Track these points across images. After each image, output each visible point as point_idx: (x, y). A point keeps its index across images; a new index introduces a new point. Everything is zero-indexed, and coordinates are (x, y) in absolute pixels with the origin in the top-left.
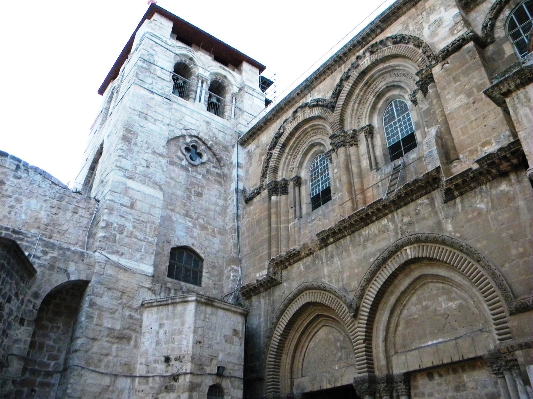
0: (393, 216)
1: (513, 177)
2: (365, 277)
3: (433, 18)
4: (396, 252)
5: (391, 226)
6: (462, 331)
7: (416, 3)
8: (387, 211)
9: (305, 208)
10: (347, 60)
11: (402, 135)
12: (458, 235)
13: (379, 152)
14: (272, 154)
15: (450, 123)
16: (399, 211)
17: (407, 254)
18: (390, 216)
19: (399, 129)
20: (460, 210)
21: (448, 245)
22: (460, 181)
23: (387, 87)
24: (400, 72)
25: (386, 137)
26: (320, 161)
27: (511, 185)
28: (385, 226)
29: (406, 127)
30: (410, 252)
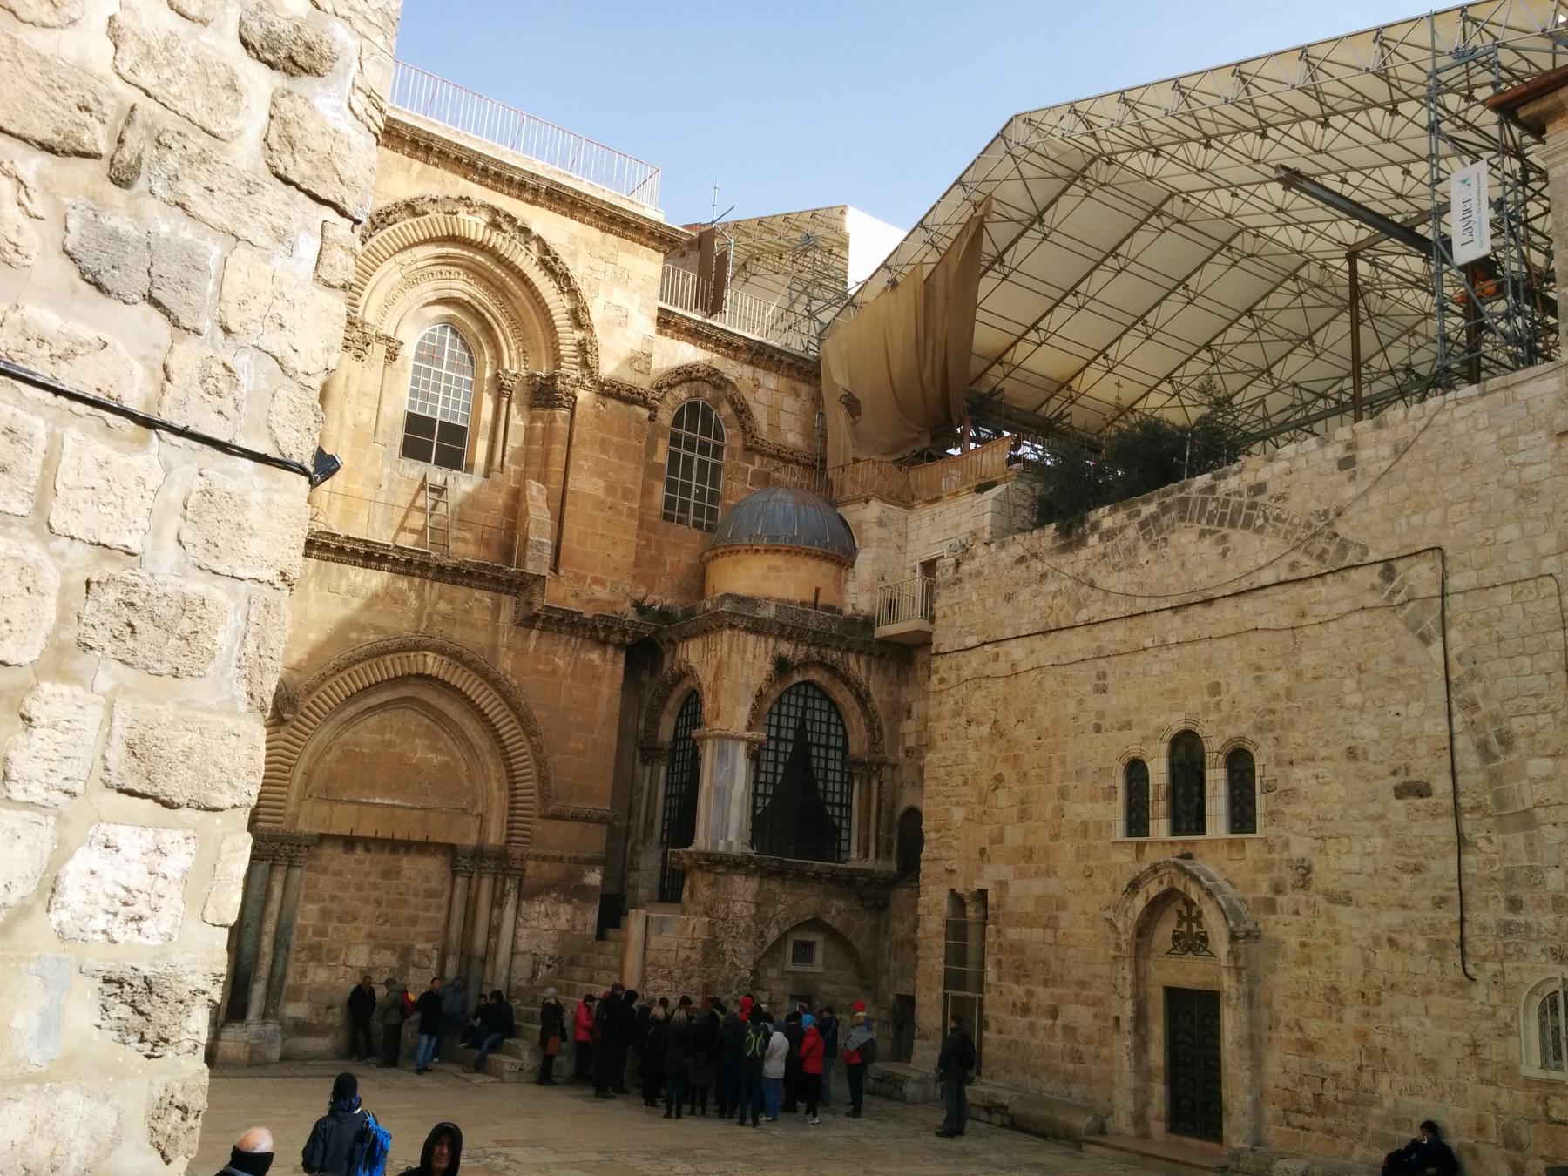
0: (422, 586)
1: (610, 650)
2: (336, 662)
3: (619, 296)
4: (411, 650)
5: (413, 600)
6: (434, 801)
7: (610, 231)
8: (417, 572)
10: (436, 165)
11: (444, 413)
12: (515, 683)
15: (568, 508)
16: (437, 584)
17: (425, 663)
18: (417, 581)
19: (441, 395)
20: (531, 649)
21: (498, 691)
22: (558, 616)
23: (468, 303)
24: (508, 308)
25: (409, 386)
27: (604, 660)
28: (401, 591)
30: (432, 664)
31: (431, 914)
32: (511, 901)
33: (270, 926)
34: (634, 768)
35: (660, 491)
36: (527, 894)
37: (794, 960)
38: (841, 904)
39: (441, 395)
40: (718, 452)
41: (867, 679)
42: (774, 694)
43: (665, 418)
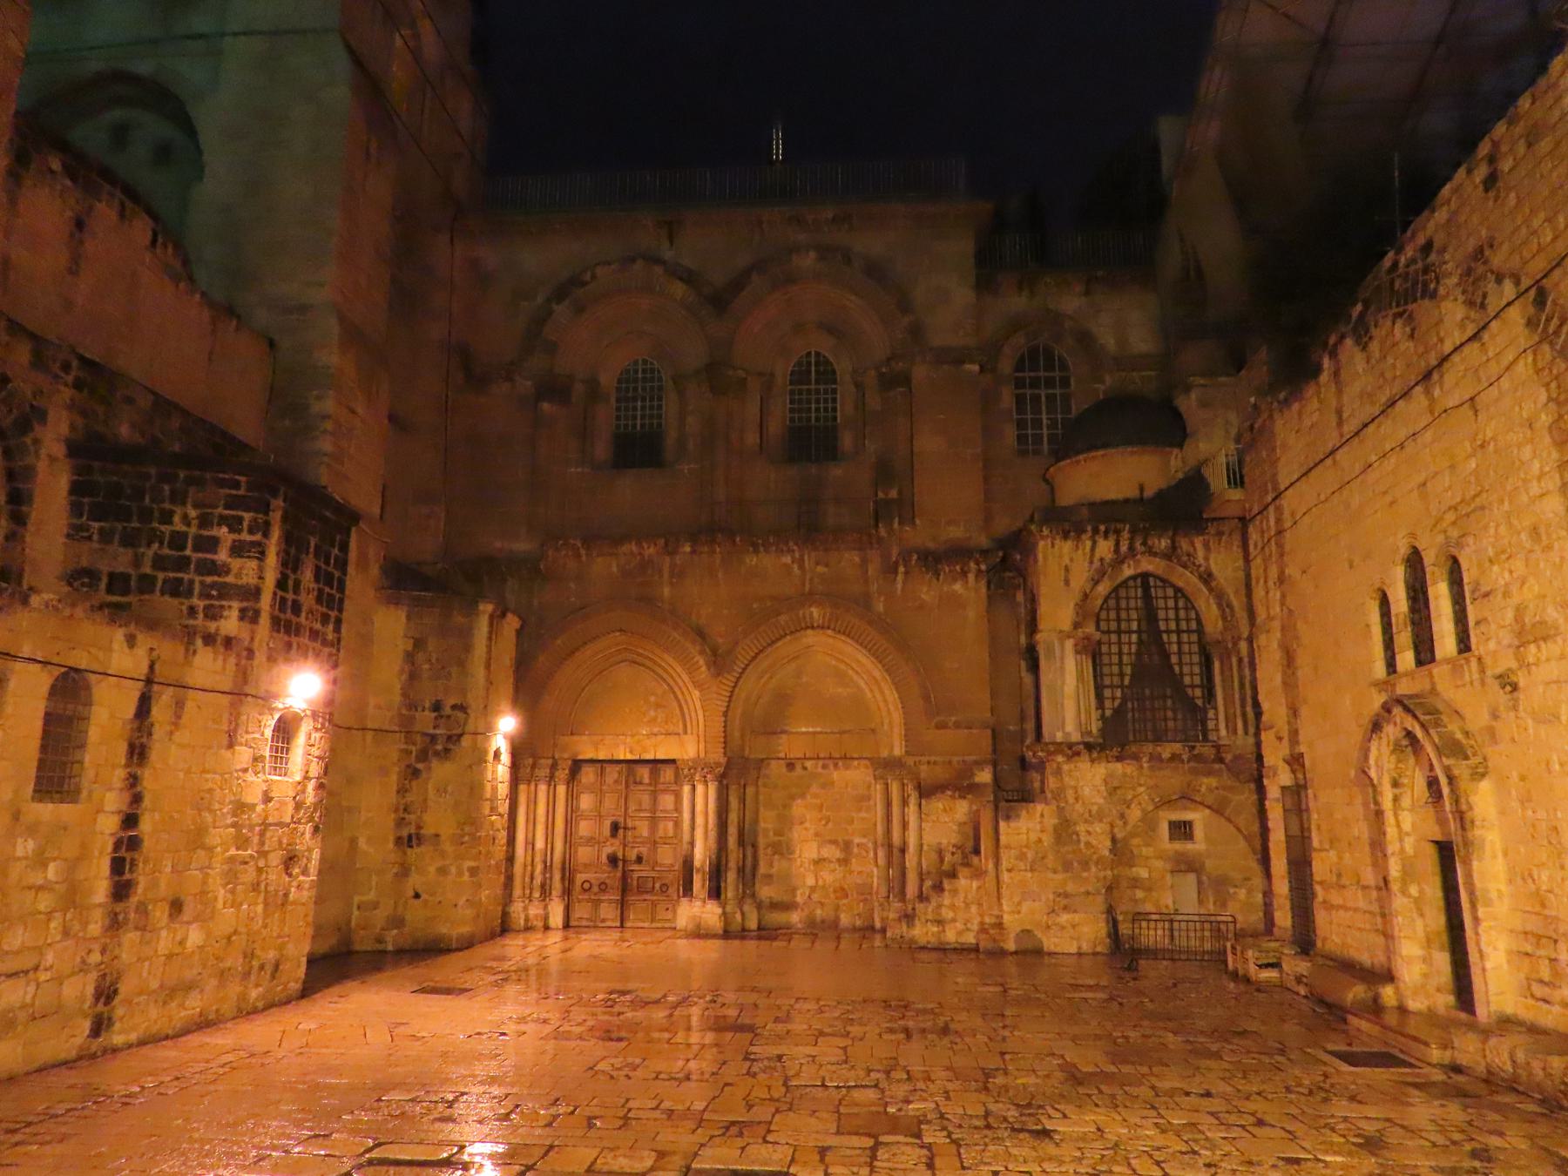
0: (802, 559)
9: (602, 449)
11: (817, 419)
13: (775, 427)
14: (550, 313)
16: (813, 554)
20: (899, 592)
26: (644, 371)
29: (826, 409)
31: (863, 815)
32: (913, 801)
33: (733, 831)
34: (1021, 678)
35: (1010, 433)
36: (926, 791)
37: (1171, 839)
38: (1212, 782)
39: (813, 406)
40: (1065, 382)
41: (1207, 559)
42: (1103, 589)
43: (1006, 366)
